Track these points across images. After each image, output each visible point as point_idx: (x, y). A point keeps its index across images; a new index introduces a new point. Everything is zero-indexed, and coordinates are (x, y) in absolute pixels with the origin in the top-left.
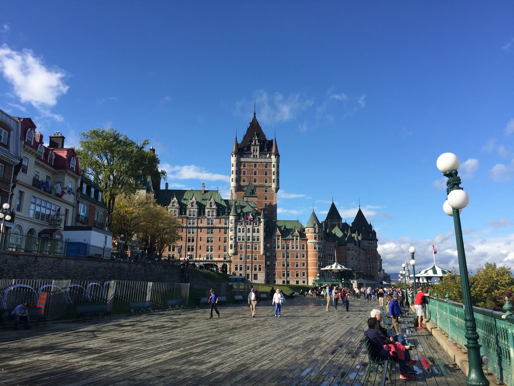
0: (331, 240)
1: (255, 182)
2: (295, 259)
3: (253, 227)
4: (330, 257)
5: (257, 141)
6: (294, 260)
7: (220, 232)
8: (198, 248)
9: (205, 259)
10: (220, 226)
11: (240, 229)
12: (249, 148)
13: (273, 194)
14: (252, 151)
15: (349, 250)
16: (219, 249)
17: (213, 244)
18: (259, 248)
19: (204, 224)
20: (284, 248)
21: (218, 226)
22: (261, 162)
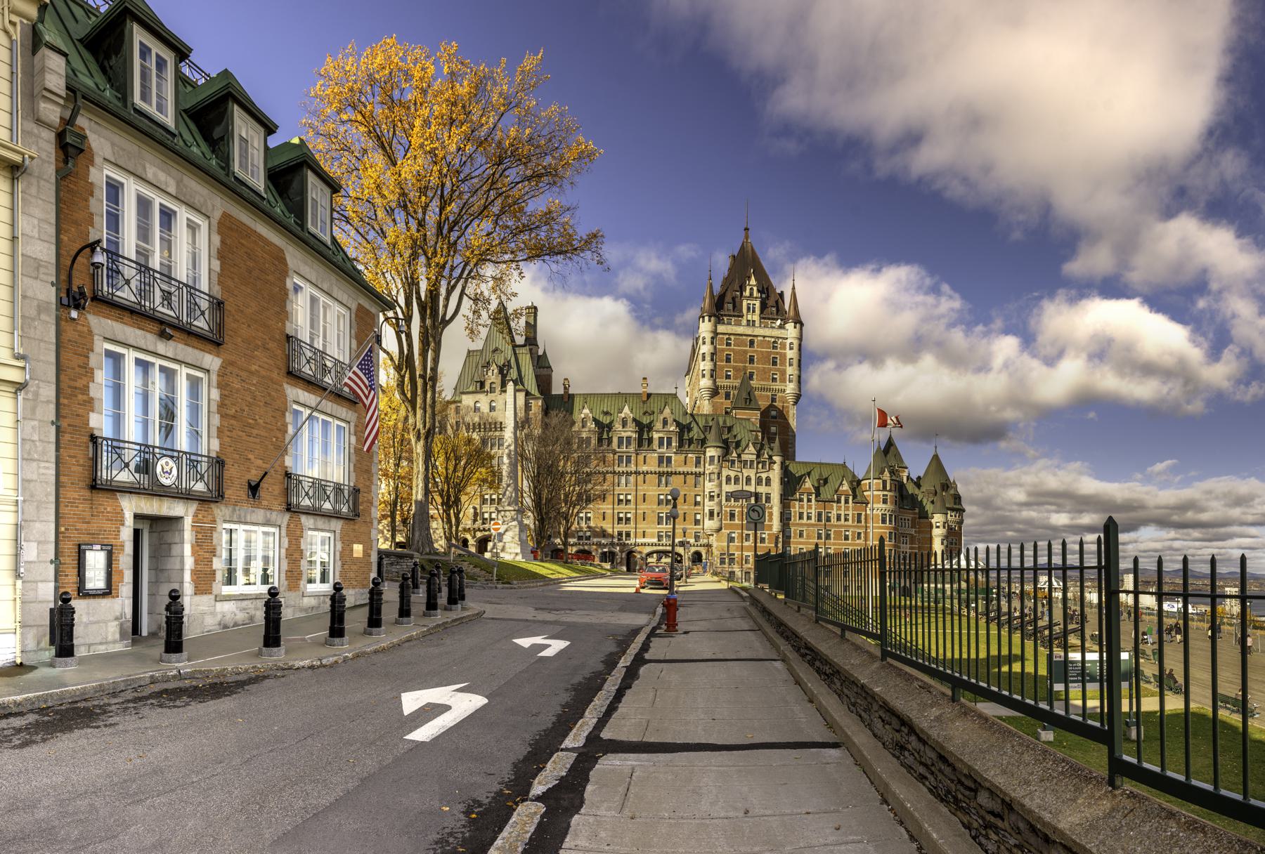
3: (757, 473)
5: (755, 288)
6: (839, 544)
8: (640, 518)
9: (655, 540)
10: (685, 469)
12: (736, 306)
14: (745, 311)
20: (820, 520)
21: (681, 469)
22: (764, 337)
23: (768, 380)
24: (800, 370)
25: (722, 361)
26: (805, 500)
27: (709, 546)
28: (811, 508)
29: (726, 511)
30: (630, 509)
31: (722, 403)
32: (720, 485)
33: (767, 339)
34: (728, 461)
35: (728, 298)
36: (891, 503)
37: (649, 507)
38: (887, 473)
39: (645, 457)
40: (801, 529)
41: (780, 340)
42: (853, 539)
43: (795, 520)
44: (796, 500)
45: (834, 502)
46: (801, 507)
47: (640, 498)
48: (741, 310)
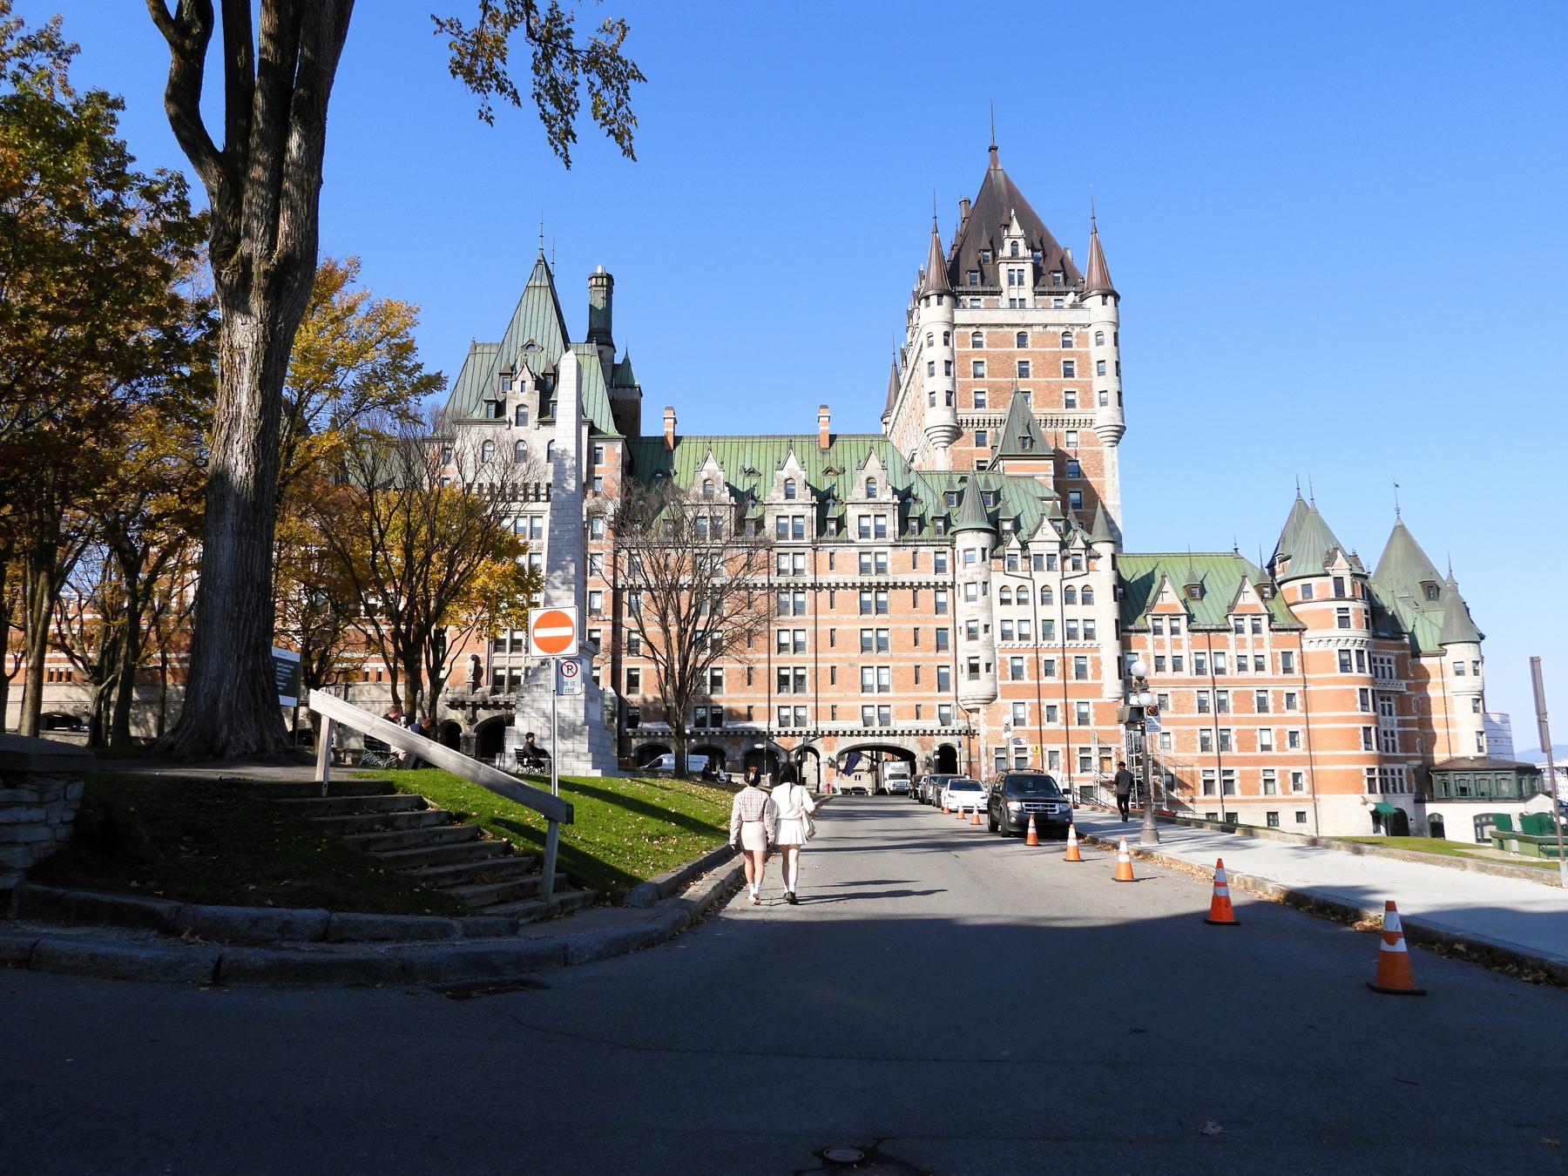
0: (1384, 631)
2: (1257, 715)
4: (1386, 703)
5: (1021, 243)
8: (825, 678)
9: (858, 725)
11: (1003, 589)
17: (886, 659)
18: (1098, 673)
19: (847, 572)
23: (1057, 404)
25: (966, 375)
26: (1166, 630)
29: (1003, 660)
30: (805, 660)
31: (971, 453)
32: (989, 607)
34: (1003, 557)
35: (969, 262)
36: (1359, 626)
37: (843, 655)
39: (832, 554)
41: (1077, 329)
42: (1278, 709)
46: (1160, 645)
47: (824, 639)
48: (997, 282)
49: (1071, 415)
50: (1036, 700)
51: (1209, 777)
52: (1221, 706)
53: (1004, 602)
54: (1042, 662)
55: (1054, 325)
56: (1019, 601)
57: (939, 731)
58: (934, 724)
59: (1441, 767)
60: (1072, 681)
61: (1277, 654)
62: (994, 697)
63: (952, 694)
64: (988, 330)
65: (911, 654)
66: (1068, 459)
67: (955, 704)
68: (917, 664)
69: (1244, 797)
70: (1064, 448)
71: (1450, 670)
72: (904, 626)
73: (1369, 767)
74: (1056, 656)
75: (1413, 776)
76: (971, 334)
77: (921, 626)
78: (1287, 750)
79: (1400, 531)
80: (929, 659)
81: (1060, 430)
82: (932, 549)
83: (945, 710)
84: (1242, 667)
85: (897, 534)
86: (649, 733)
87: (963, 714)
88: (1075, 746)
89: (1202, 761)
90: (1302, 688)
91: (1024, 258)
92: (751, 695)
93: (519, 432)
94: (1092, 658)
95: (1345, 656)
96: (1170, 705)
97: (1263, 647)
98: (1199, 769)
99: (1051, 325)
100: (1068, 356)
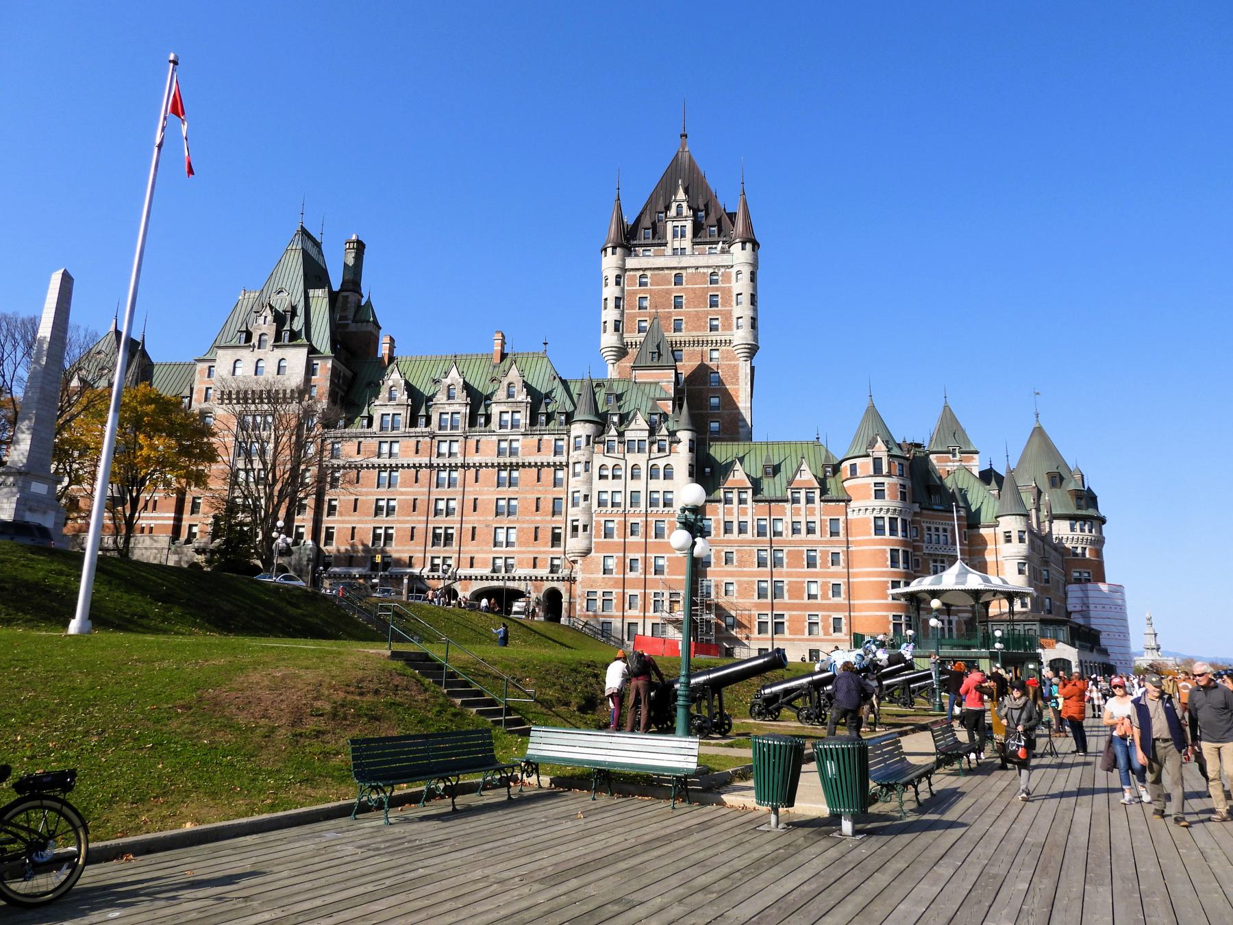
0: (941, 505)
1: (677, 329)
2: (806, 569)
4: (939, 564)
5: (685, 205)
7: (539, 480)
9: (487, 571)
10: (539, 459)
11: (602, 467)
13: (736, 366)
15: (1008, 539)
16: (536, 539)
17: (513, 522)
19: (488, 455)
20: (761, 533)
21: (532, 459)
22: (697, 268)
23: (702, 328)
24: (755, 310)
27: (571, 580)
28: (745, 514)
29: (598, 523)
32: (590, 481)
33: (701, 270)
34: (603, 443)
35: (646, 222)
36: (893, 497)
37: (481, 518)
38: (880, 445)
39: (478, 441)
40: (729, 550)
41: (722, 270)
42: (824, 565)
43: (718, 535)
44: (719, 501)
45: (787, 501)
46: (730, 512)
47: (469, 505)
48: (665, 236)
49: (714, 336)
50: (622, 555)
51: (763, 619)
52: (777, 563)
53: (601, 477)
54: (629, 525)
55: (704, 267)
56: (614, 477)
57: (547, 578)
58: (543, 572)
59: (995, 618)
60: (652, 540)
61: (826, 520)
62: (589, 551)
63: (562, 549)
64: (652, 272)
65: (533, 518)
66: (710, 371)
67: (563, 557)
68: (537, 525)
69: (791, 637)
70: (707, 362)
71: (1001, 538)
72: (529, 496)
73: (895, 614)
74: (640, 520)
75: (964, 627)
76: (638, 276)
77: (542, 496)
78: (830, 599)
79: (1039, 431)
80: (546, 522)
81: (705, 348)
82: (553, 437)
83: (556, 562)
84: (795, 531)
85: (527, 425)
86: (335, 575)
87: (569, 565)
88: (652, 591)
89: (757, 606)
90: (845, 549)
91: (686, 217)
92: (412, 548)
93: (258, 353)
94: (668, 521)
95: (880, 523)
96: (735, 561)
97: (814, 515)
98: (755, 613)
99: (701, 267)
100: (713, 291)
